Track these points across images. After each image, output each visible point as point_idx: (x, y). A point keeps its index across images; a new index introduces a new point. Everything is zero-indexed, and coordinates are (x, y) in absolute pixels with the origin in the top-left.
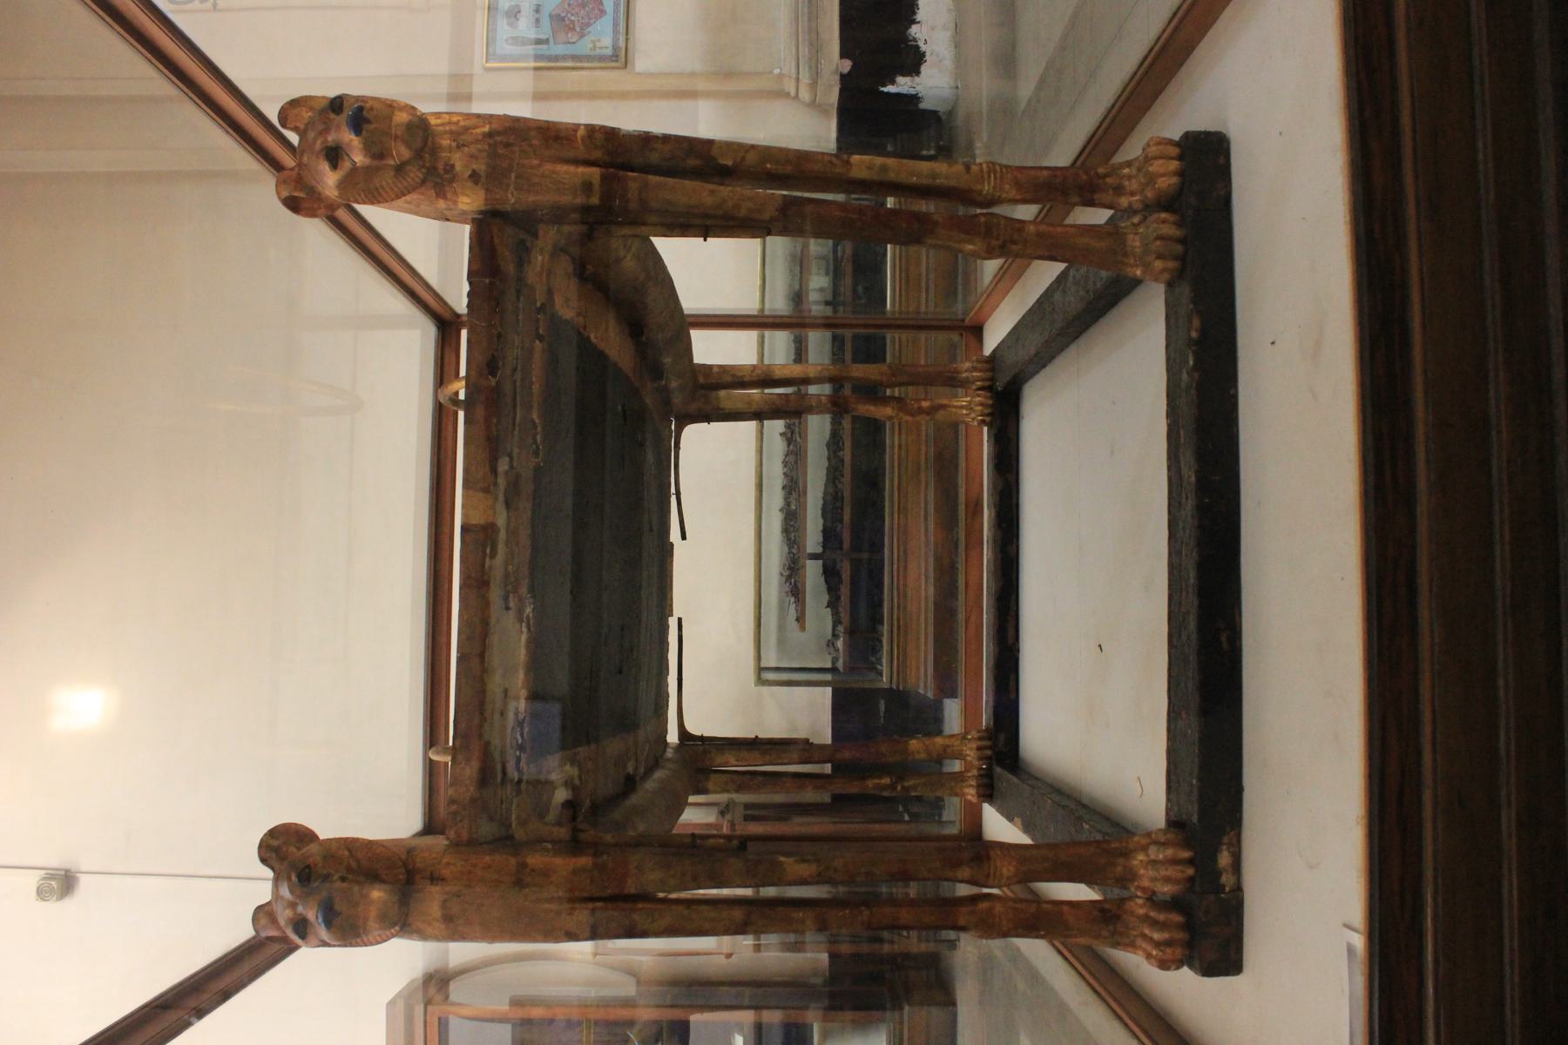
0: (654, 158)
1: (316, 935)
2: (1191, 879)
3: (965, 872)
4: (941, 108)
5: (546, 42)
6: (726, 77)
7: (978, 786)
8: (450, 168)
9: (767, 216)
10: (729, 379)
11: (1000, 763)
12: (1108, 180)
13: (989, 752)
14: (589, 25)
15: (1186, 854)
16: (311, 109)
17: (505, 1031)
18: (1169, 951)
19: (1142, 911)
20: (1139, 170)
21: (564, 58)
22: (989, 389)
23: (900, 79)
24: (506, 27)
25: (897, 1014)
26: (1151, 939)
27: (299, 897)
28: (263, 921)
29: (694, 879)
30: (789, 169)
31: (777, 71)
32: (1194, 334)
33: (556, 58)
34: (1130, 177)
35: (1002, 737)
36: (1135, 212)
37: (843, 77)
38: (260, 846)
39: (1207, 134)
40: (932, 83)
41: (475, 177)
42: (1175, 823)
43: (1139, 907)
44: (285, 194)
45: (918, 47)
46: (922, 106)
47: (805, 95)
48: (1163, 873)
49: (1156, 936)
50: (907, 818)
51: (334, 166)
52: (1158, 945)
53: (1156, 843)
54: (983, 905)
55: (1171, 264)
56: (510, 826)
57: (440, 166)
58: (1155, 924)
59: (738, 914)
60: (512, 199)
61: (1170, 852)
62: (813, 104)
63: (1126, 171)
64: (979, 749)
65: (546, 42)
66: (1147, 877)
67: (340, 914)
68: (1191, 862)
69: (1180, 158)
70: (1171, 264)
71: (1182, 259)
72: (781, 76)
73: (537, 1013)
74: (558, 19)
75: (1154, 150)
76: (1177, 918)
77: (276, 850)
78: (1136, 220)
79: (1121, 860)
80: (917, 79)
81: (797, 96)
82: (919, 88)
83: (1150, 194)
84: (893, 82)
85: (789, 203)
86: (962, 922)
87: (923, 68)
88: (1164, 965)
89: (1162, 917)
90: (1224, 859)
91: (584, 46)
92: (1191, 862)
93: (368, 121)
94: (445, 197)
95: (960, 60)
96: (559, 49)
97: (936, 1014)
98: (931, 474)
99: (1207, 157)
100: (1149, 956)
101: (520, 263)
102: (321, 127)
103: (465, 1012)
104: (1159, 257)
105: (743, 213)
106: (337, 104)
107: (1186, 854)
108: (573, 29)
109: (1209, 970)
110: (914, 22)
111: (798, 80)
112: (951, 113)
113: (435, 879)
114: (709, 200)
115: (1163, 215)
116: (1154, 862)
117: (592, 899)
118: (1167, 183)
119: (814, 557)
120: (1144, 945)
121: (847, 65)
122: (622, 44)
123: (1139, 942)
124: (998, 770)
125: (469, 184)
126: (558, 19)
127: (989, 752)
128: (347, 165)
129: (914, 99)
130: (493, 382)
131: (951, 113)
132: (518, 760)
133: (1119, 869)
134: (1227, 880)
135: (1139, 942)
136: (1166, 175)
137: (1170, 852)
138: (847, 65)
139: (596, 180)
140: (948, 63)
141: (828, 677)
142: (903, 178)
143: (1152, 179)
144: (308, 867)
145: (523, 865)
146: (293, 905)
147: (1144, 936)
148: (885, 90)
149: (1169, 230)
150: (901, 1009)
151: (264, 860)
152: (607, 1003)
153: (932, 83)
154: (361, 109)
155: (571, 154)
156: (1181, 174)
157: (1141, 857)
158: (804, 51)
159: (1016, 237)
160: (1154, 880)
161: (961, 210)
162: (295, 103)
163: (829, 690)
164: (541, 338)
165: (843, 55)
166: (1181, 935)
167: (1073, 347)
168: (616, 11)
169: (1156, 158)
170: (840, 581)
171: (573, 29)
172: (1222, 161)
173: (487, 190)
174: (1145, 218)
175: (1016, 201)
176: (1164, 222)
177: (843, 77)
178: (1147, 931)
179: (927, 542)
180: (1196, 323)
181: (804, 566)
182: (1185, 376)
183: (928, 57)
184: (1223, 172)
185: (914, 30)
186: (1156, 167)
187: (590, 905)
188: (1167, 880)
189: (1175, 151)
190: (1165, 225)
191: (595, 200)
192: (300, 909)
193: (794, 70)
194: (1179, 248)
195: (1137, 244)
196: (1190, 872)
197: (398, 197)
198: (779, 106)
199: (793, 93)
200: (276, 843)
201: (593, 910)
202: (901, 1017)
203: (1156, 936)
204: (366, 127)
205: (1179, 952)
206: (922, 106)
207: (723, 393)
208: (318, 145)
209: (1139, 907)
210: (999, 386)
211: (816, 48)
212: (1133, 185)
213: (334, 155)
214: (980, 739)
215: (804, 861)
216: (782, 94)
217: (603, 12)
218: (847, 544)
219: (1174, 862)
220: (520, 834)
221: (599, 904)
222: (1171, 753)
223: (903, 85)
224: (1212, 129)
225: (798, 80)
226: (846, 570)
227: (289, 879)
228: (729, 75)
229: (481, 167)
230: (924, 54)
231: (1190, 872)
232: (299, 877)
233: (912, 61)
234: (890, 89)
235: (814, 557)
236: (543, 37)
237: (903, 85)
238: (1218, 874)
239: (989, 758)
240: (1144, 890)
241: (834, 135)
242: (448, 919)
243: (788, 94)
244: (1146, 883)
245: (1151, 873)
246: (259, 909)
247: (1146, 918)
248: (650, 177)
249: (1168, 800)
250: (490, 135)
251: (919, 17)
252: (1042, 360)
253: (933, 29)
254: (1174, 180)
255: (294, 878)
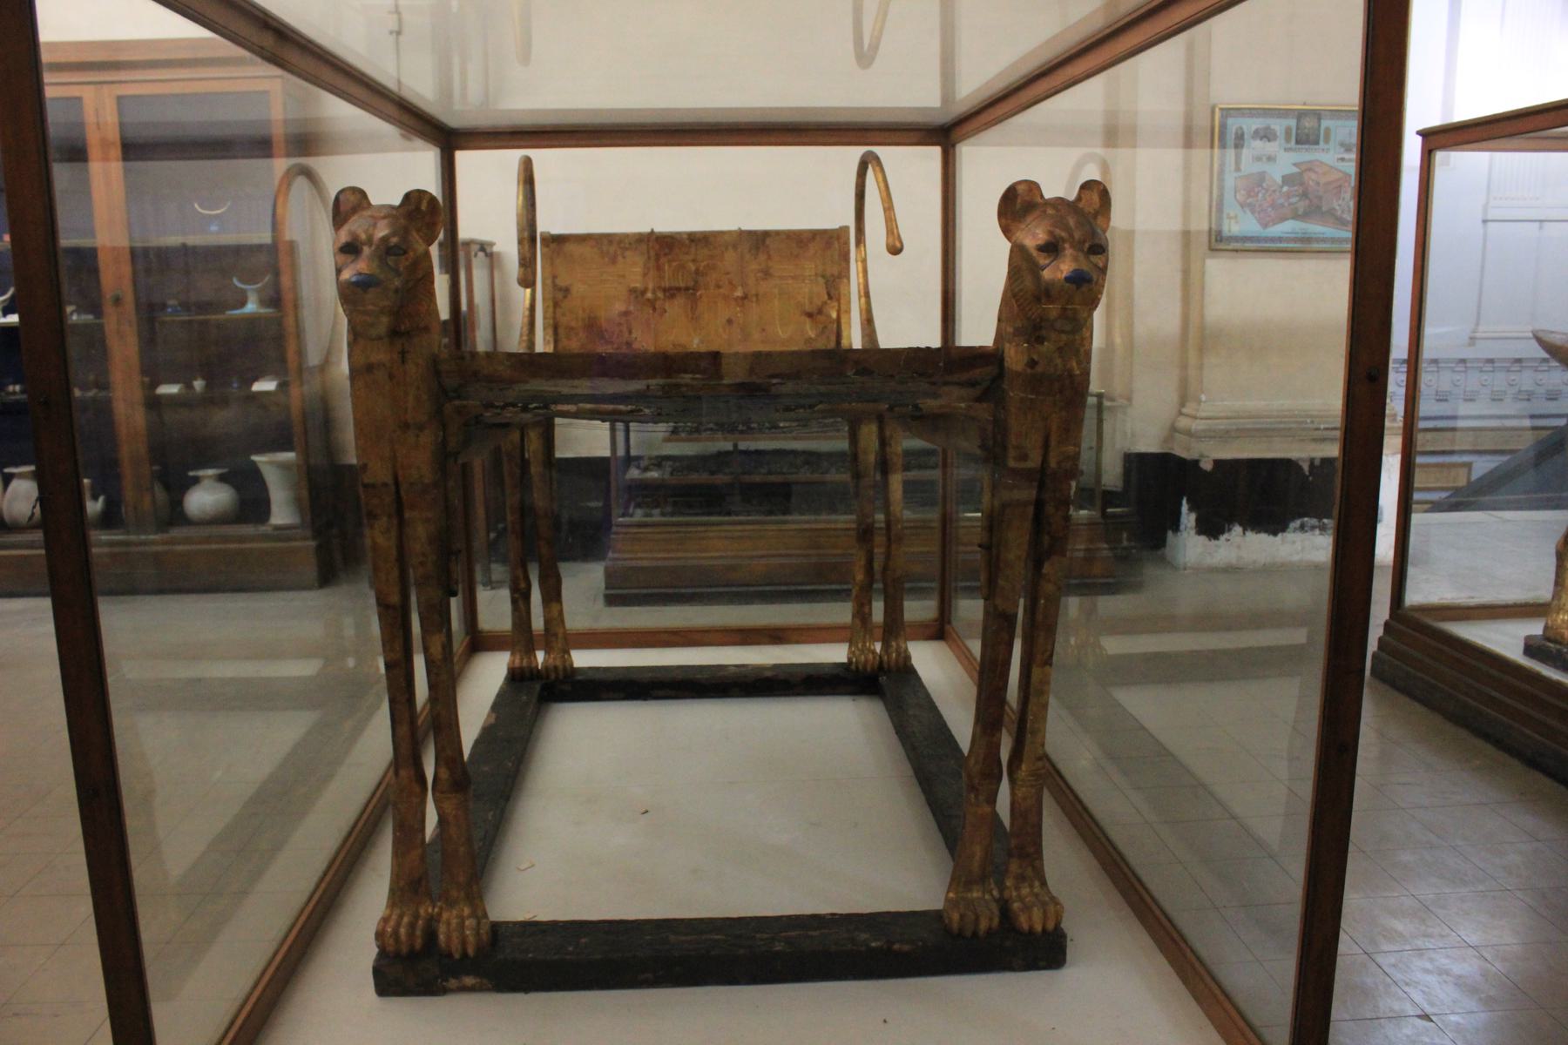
0: (1050, 509)
1: (345, 265)
2: (450, 955)
3: (444, 774)
4: (1167, 551)
5: (1238, 169)
6: (1198, 340)
7: (521, 669)
8: (1040, 340)
9: (998, 601)
10: (888, 433)
11: (543, 688)
12: (1029, 872)
13: (553, 676)
14: (1253, 212)
15: (471, 951)
16: (1096, 215)
17: (265, 237)
18: (391, 941)
19: (422, 911)
20: (1037, 895)
21: (1221, 188)
22: (881, 668)
23: (1193, 517)
24: (1254, 128)
25: (309, 533)
26: (398, 924)
27: (378, 247)
28: (352, 198)
29: (422, 564)
30: (1039, 617)
31: (1203, 398)
32: (896, 947)
33: (1221, 180)
34: (1031, 886)
35: (567, 688)
36: (1001, 891)
37: (1196, 462)
38: (419, 191)
39: (1064, 953)
40: (1190, 545)
41: (1032, 363)
42: (498, 931)
43: (426, 910)
44: (1020, 188)
45: (1223, 533)
46: (1170, 533)
47: (1183, 423)
48: (455, 935)
49: (402, 931)
50: (492, 535)
51: (1041, 249)
52: (396, 933)
53: (479, 923)
54: (417, 789)
55: (955, 926)
56: (459, 397)
57: (1044, 332)
58: (412, 926)
59: (395, 599)
60: (1015, 394)
61: (471, 939)
62: (1174, 429)
63: (1037, 884)
64: (556, 668)
65: (1238, 169)
66: (450, 917)
67: (365, 291)
68: (465, 955)
69: (1044, 930)
70: (955, 926)
71: (960, 935)
72: (1199, 402)
73: (284, 262)
74: (1262, 177)
75: (1051, 908)
76: (418, 943)
77: (418, 209)
78: (995, 893)
79: (462, 894)
80: (1193, 532)
81: (1181, 414)
82: (1185, 534)
83: (1016, 905)
84: (1191, 510)
85: (1010, 620)
86: (403, 773)
87: (1203, 539)
88: (379, 935)
89: (418, 933)
90: (469, 981)
91: (1231, 207)
92: (465, 955)
93: (1079, 287)
94: (1014, 335)
95: (1213, 570)
96: (1230, 181)
97: (311, 572)
98: (814, 560)
99: (1044, 950)
100: (385, 920)
101: (961, 384)
102: (1077, 235)
103: (279, 211)
104: (962, 917)
105: (1001, 582)
106: (1098, 248)
107: (471, 951)
108: (1249, 196)
109: (377, 972)
110: (1245, 530)
111: (1195, 418)
112: (1164, 562)
113: (403, 353)
114: (1011, 556)
115: (996, 921)
116: (462, 926)
117: (397, 483)
118: (1023, 922)
119: (735, 446)
120: (394, 917)
121: (1207, 466)
122: (1233, 245)
123: (397, 912)
124: (538, 687)
125: (1025, 359)
126: (1262, 177)
127: (553, 676)
128: (1042, 260)
129: (1176, 527)
130: (849, 373)
131: (1164, 562)
132: (514, 405)
133: (454, 893)
134: (453, 983)
135: (397, 912)
136: (1033, 920)
137: (471, 939)
138: (1207, 466)
139: (1030, 464)
140: (1210, 561)
141: (621, 452)
142: (1032, 707)
143: (1027, 908)
144: (405, 252)
145: (421, 428)
146: (369, 241)
147: (401, 917)
148: (1184, 501)
149: (983, 925)
150: (314, 538)
151: (407, 196)
152: (299, 334)
153: (1190, 545)
154: (1089, 281)
155: (1053, 443)
156: (1031, 928)
157: (467, 911)
158: (1222, 425)
159: (981, 798)
160: (448, 924)
161: (1005, 756)
162: (1105, 196)
163: (607, 453)
164: (891, 409)
165: (1217, 463)
166: (404, 949)
167: (911, 772)
168: (1266, 239)
169: (1045, 913)
170: (712, 473)
171: (1249, 196)
172: (1042, 964)
173: (1018, 374)
174: (997, 901)
175: (1013, 794)
176: (991, 919)
177: (1196, 462)
178: (406, 920)
179: (752, 557)
180: (906, 948)
181: (725, 439)
182: (864, 936)
183: (1214, 542)
184: (1031, 965)
185: (1238, 529)
186: (1037, 914)
187: (389, 480)
188: (449, 938)
189: (1050, 926)
190: (988, 920)
191: (1012, 463)
192: (366, 250)
193: (1204, 414)
194: (968, 933)
195: (975, 895)
196: (457, 956)
197: (1014, 296)
198: (1172, 397)
199: (1184, 410)
200: (424, 207)
201: (385, 485)
202: (305, 539)
203: (402, 931)
204: (1074, 287)
205: (390, 949)
206: (1170, 533)
207: (874, 428)
208: (1058, 232)
209: (426, 910)
210: (883, 679)
211: (1225, 436)
212: (1025, 891)
213: (1052, 248)
214: (565, 669)
215: (444, 648)
216: (1183, 401)
217: (1265, 226)
218: (747, 478)
219: (464, 942)
220: (449, 408)
221: (393, 488)
222: (554, 926)
223: (1188, 519)
224: (1068, 957)
225: (1195, 418)
226: (721, 479)
227: (394, 234)
228: (1201, 350)
229: (1039, 369)
230: (1216, 538)
231: (457, 956)
232: (396, 246)
233: (1211, 528)
234: (1185, 507)
235: (735, 446)
236: (1243, 167)
237: (1188, 519)
238: (456, 975)
239: (548, 677)
240: (440, 914)
241: (1142, 447)
242: (370, 368)
243: (1182, 404)
244: (445, 916)
245: (454, 922)
246: (361, 194)
247: (416, 916)
248: (1031, 510)
249: (515, 923)
250: (1071, 376)
251: (1249, 534)
252: (902, 731)
253: (1239, 547)
254: (1025, 927)
255: (394, 240)
